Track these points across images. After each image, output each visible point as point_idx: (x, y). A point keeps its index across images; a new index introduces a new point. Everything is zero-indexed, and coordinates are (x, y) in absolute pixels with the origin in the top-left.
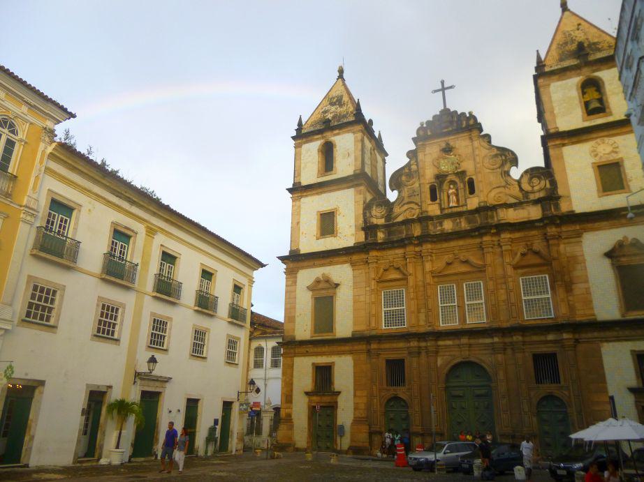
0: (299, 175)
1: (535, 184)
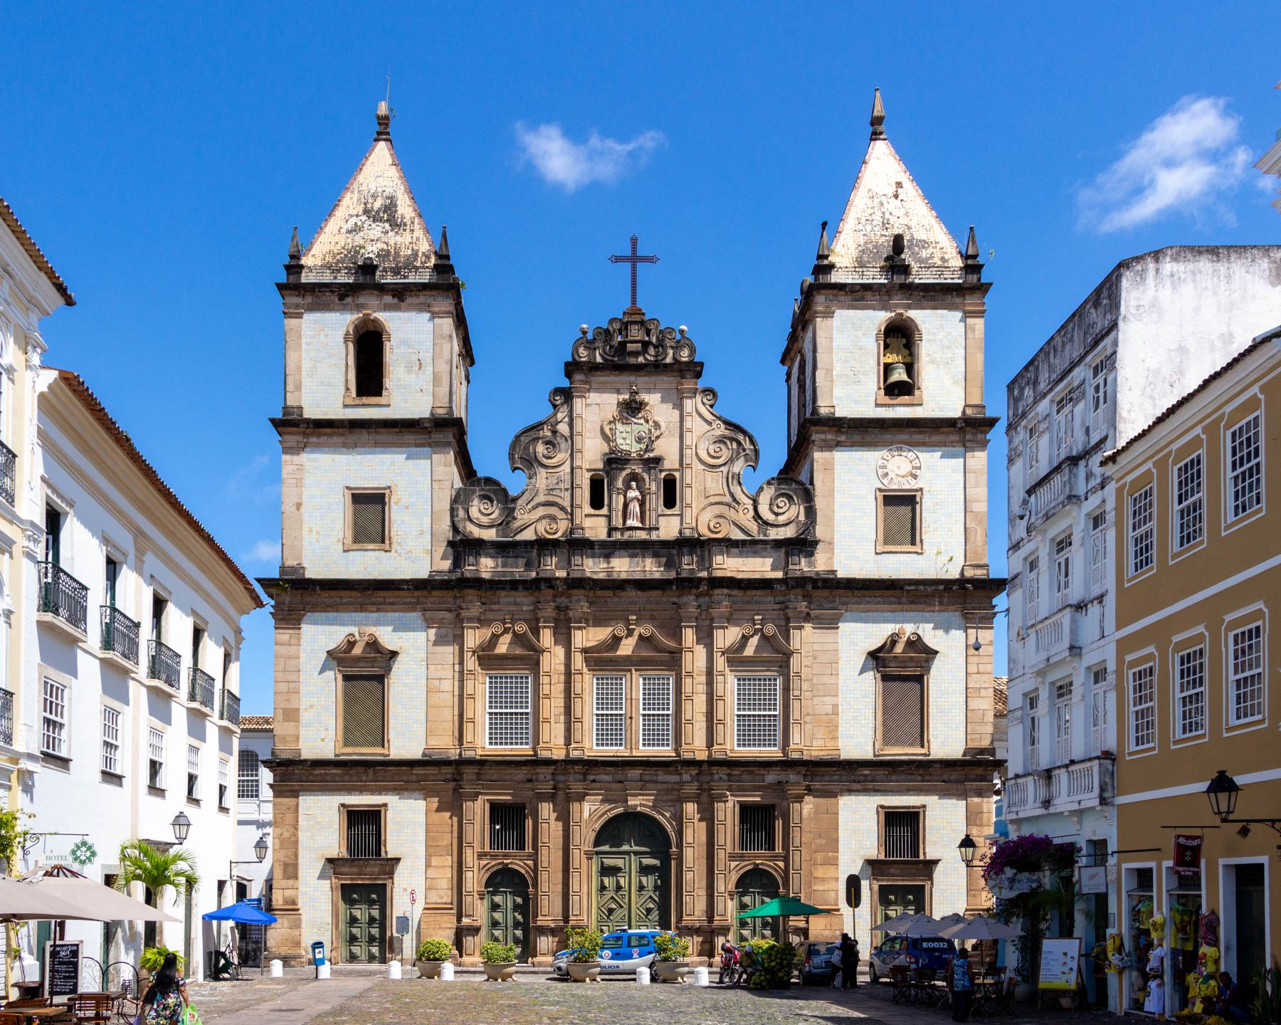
0: (299, 387)
1: (781, 511)
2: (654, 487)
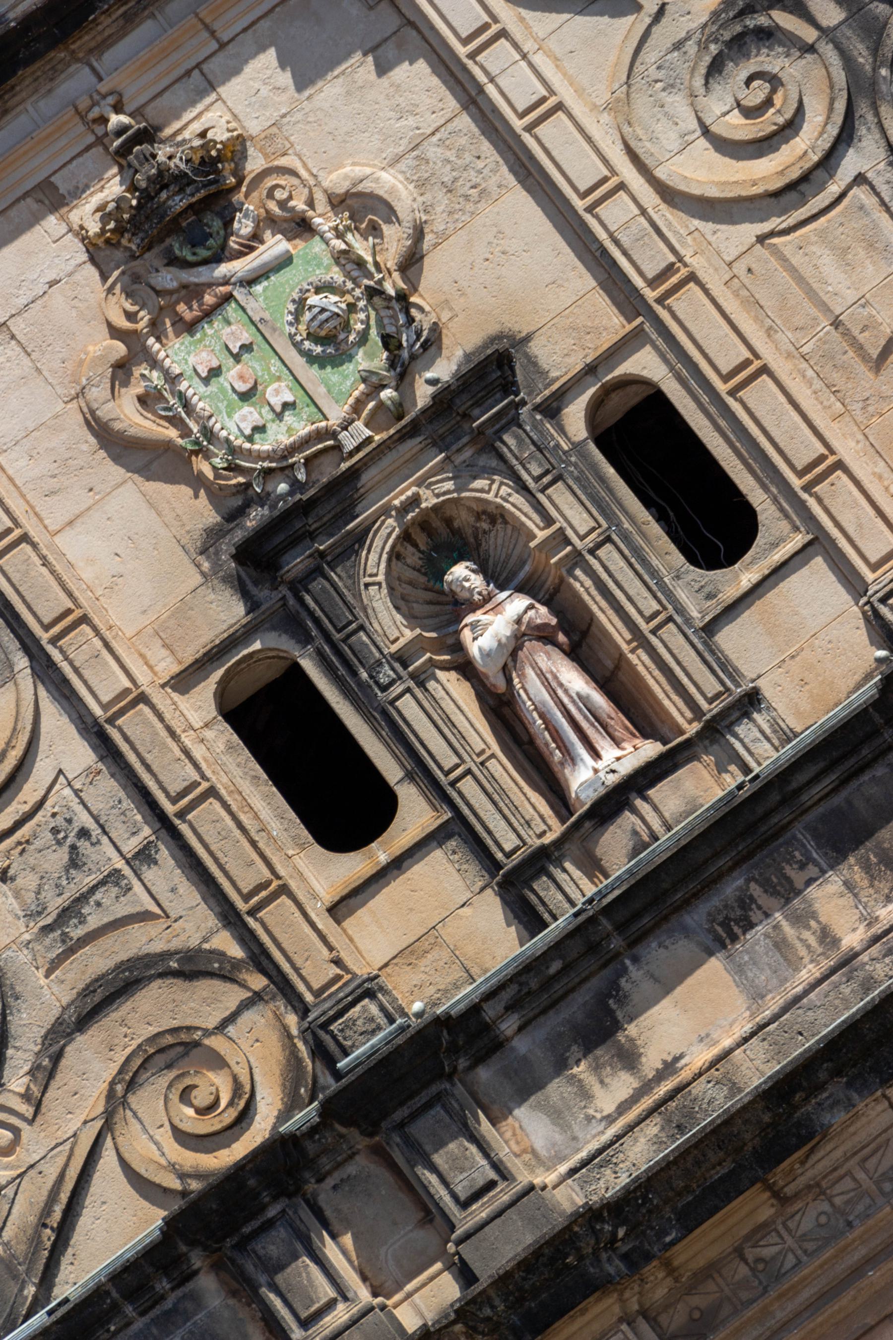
2: (575, 509)
